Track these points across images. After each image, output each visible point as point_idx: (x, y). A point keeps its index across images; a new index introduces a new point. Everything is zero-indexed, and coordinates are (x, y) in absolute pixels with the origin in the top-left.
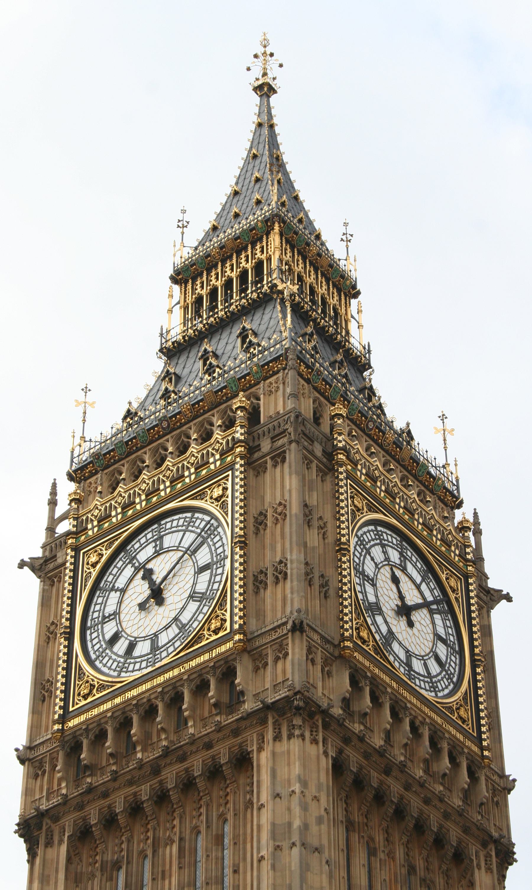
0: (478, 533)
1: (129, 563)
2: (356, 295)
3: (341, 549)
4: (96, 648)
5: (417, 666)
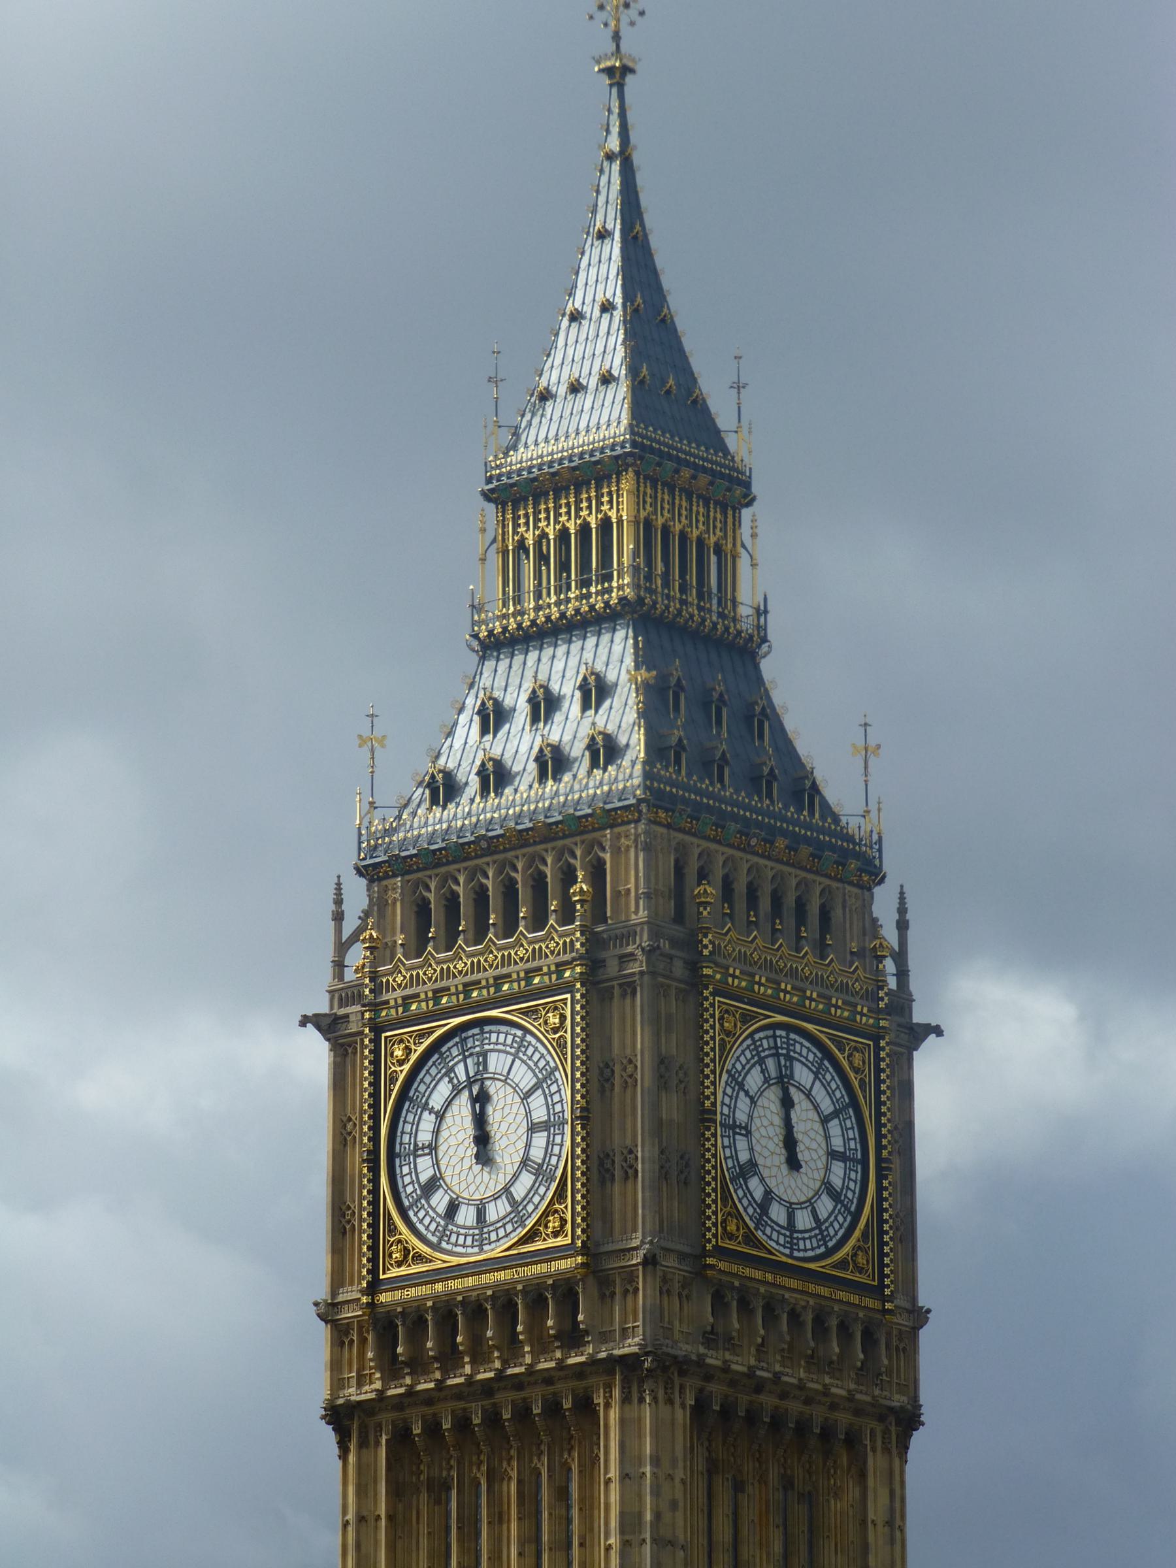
0: (902, 926)
1: (445, 1074)
2: (749, 504)
3: (705, 1117)
4: (409, 1189)
5: (803, 1220)
